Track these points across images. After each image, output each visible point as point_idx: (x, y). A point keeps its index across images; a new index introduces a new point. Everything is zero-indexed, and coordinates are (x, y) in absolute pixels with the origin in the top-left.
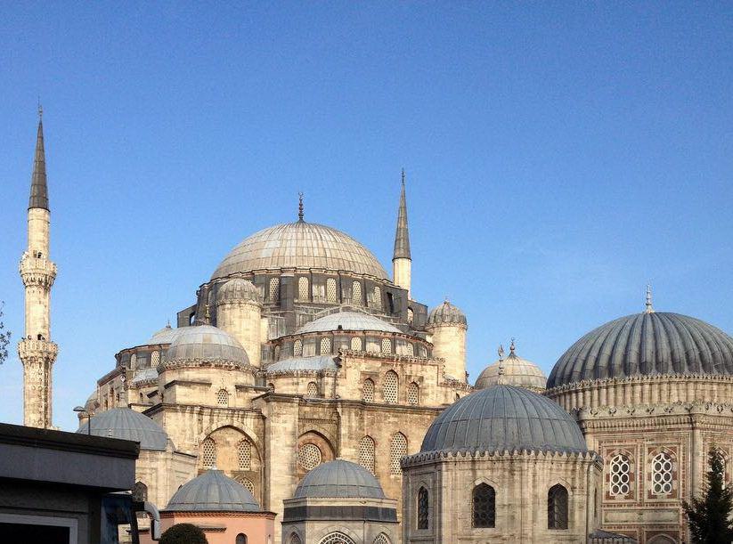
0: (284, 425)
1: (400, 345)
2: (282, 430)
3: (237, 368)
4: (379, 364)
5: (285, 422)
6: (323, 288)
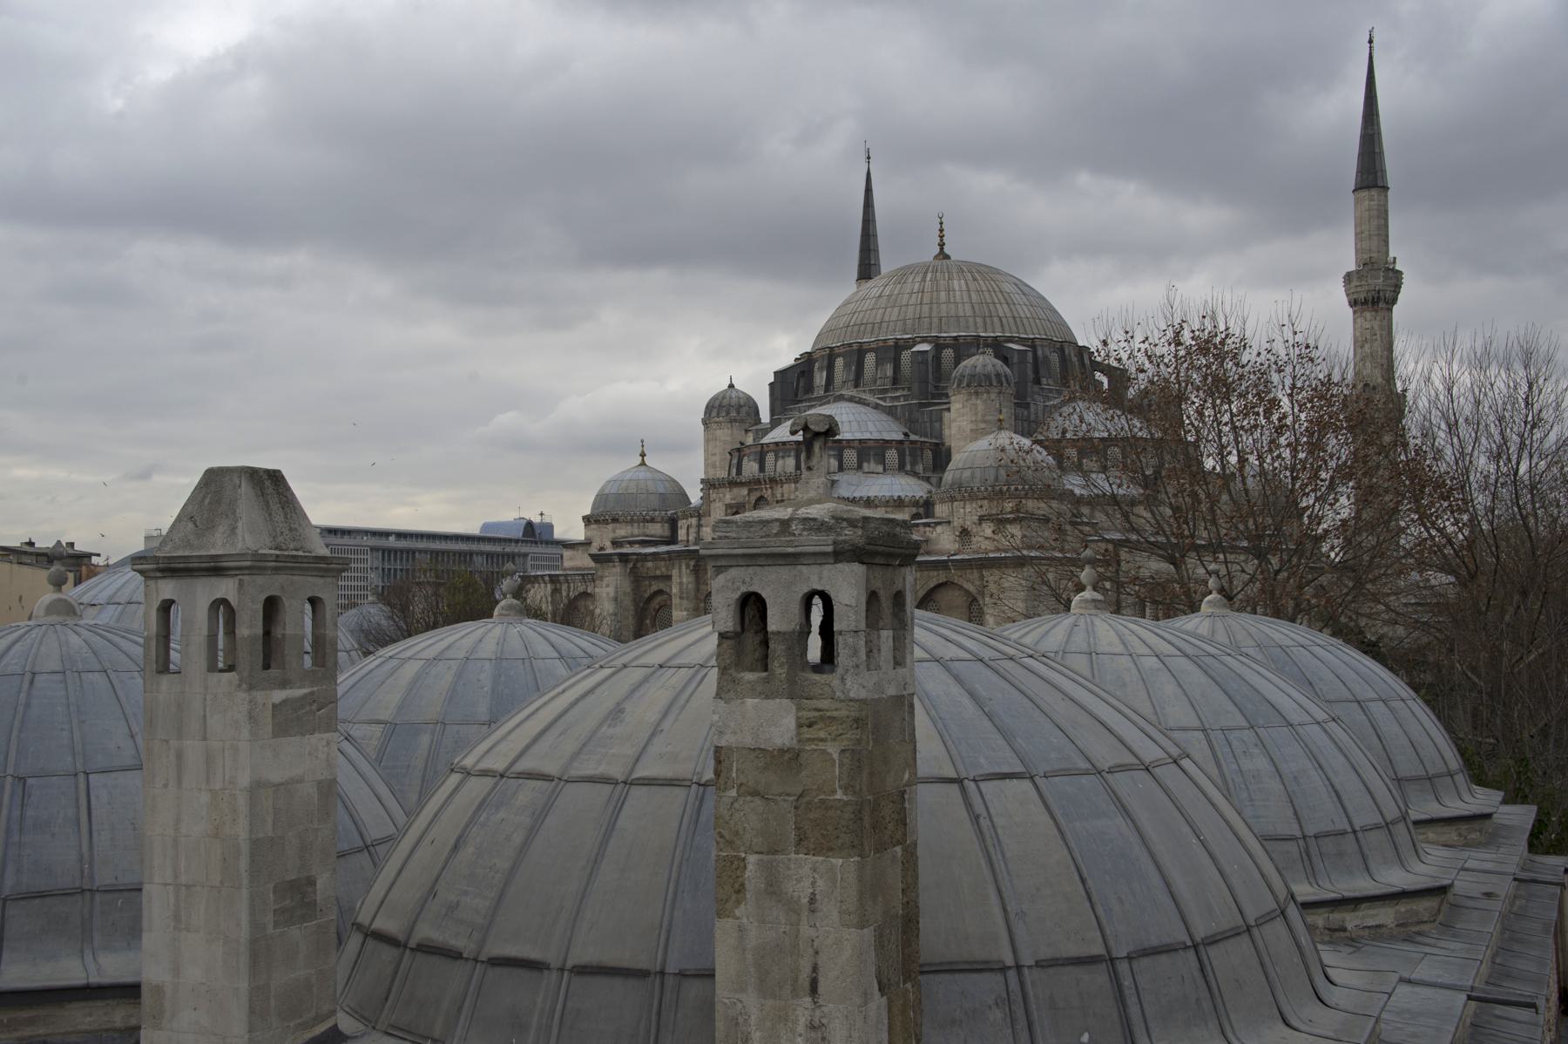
0: (608, 589)
1: (783, 457)
2: (605, 595)
3: (615, 520)
4: (745, 491)
5: (608, 586)
6: (825, 373)
